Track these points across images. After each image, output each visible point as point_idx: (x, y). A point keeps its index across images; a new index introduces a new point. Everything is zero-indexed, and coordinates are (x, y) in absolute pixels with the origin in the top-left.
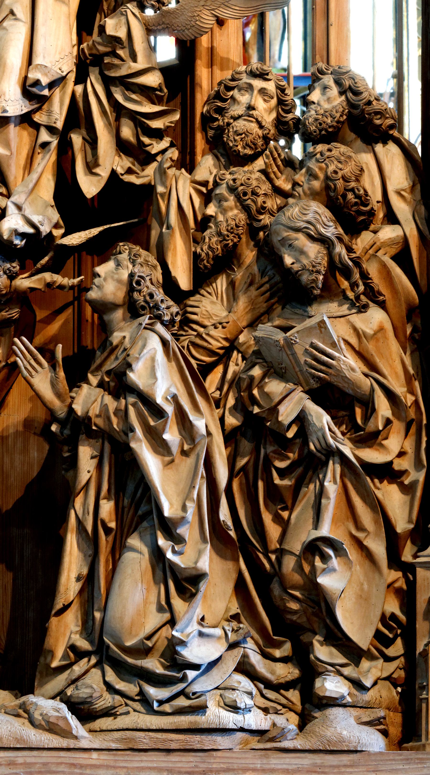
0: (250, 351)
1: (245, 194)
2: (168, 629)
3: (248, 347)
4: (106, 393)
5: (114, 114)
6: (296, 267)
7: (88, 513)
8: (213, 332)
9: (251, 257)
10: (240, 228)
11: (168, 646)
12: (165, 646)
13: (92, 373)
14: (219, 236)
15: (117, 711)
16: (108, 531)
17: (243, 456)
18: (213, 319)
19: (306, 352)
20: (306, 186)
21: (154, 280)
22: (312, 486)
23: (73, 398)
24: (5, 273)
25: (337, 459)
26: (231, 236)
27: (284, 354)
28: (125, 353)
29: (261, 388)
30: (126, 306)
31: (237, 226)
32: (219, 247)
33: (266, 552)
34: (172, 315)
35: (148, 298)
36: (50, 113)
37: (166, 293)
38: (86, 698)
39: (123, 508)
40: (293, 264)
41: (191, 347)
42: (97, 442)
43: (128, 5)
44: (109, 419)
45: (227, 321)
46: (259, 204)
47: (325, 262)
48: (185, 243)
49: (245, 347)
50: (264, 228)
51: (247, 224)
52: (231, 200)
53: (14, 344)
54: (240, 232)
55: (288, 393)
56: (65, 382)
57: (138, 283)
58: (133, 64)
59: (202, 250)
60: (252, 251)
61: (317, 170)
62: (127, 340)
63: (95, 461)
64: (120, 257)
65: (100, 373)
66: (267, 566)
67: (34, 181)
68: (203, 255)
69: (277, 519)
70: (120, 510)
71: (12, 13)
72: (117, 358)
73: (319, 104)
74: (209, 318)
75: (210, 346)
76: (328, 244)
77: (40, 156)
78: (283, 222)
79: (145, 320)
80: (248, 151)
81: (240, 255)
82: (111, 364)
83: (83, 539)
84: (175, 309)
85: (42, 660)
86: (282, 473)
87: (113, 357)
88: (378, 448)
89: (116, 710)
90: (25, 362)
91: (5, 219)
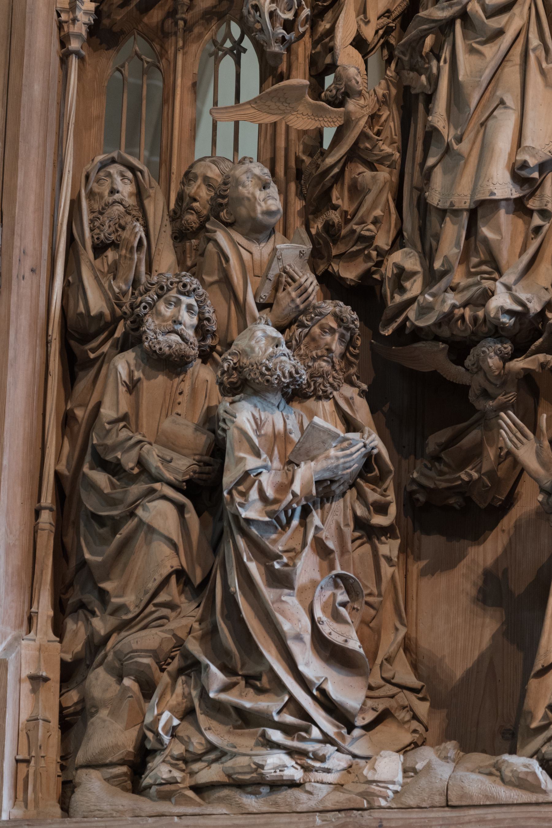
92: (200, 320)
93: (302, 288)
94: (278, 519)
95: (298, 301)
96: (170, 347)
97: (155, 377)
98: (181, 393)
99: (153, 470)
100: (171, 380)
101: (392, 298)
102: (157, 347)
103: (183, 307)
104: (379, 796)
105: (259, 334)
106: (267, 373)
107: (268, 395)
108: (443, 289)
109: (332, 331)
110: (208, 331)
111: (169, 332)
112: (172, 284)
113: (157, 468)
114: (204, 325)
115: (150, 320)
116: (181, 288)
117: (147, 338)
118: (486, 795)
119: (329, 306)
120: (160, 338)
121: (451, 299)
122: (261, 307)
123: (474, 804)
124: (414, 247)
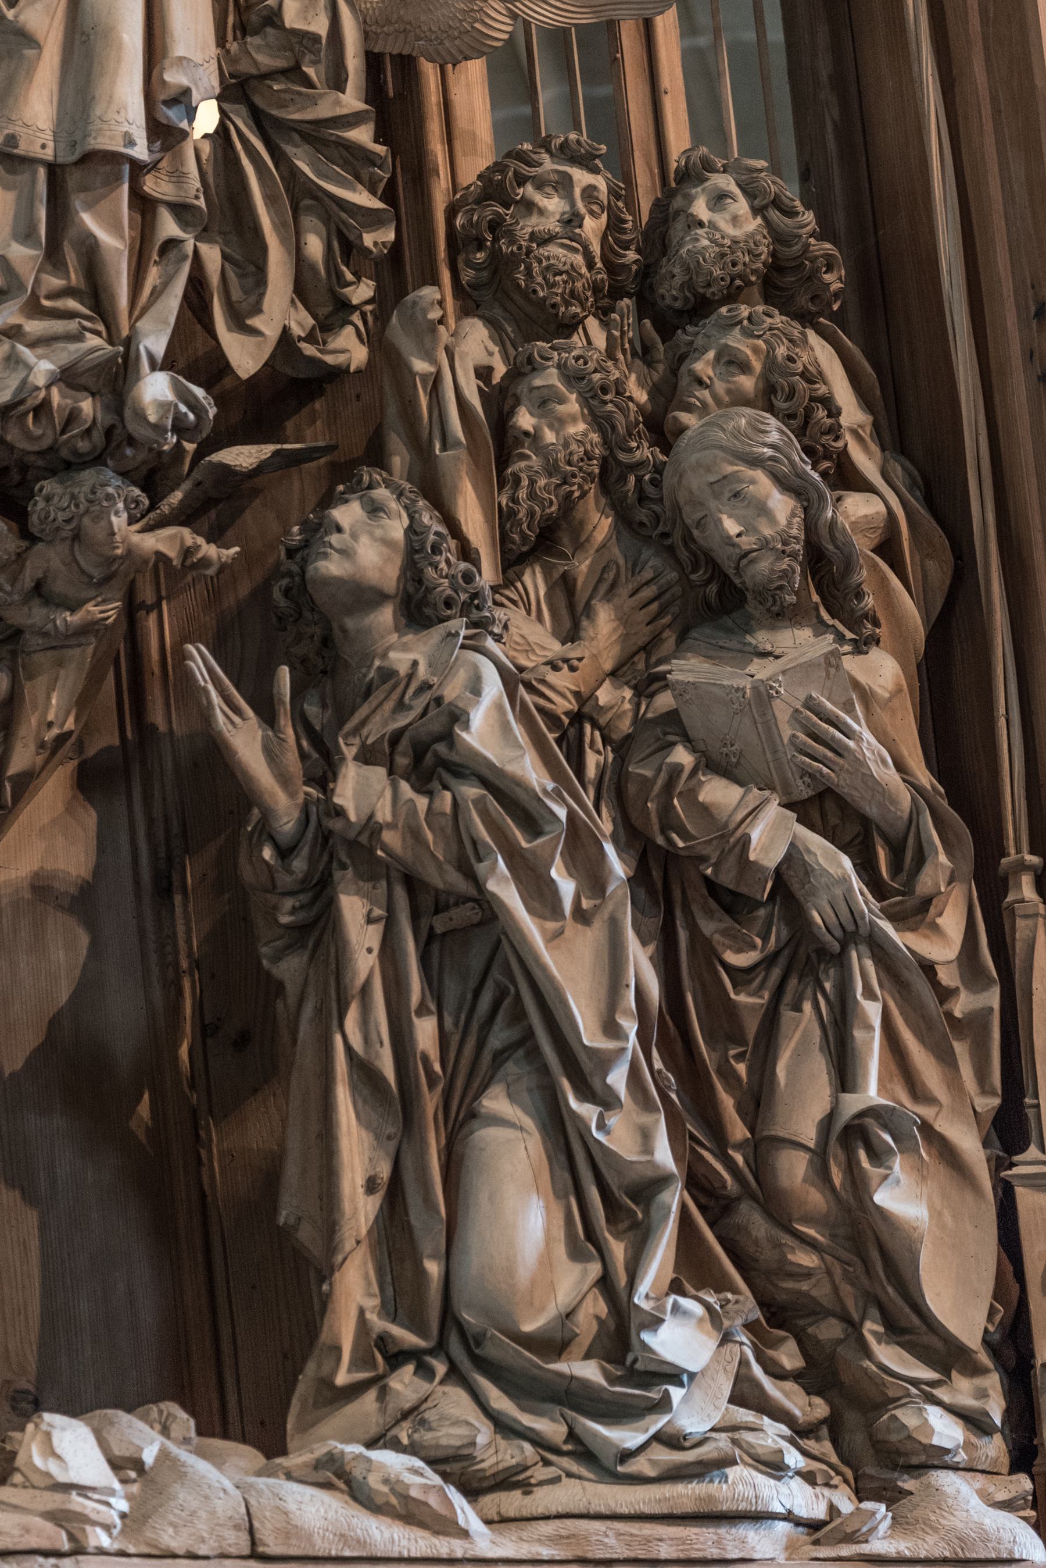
0: (625, 726)
2: (595, 1299)
3: (620, 716)
6: (747, 542)
8: (552, 677)
9: (606, 530)
10: (595, 462)
11: (598, 1335)
12: (591, 1337)
14: (550, 475)
15: (531, 1477)
18: (536, 655)
19: (796, 719)
22: (807, 1006)
24: (127, 508)
25: (864, 949)
27: (747, 721)
30: (398, 599)
32: (553, 497)
35: (461, 581)
38: (459, 1448)
40: (739, 535)
42: (374, 887)
45: (579, 656)
47: (803, 537)
49: (610, 715)
52: (572, 405)
55: (758, 803)
57: (436, 549)
60: (607, 517)
68: (522, 514)
72: (401, 706)
74: (527, 651)
75: (548, 705)
76: (808, 500)
78: (724, 443)
79: (459, 626)
81: (582, 523)
83: (365, 1102)
85: (311, 1367)
86: (741, 977)
88: (927, 932)
89: (528, 1473)
104: (95, 1523)
118: (342, 1535)
123: (315, 1554)
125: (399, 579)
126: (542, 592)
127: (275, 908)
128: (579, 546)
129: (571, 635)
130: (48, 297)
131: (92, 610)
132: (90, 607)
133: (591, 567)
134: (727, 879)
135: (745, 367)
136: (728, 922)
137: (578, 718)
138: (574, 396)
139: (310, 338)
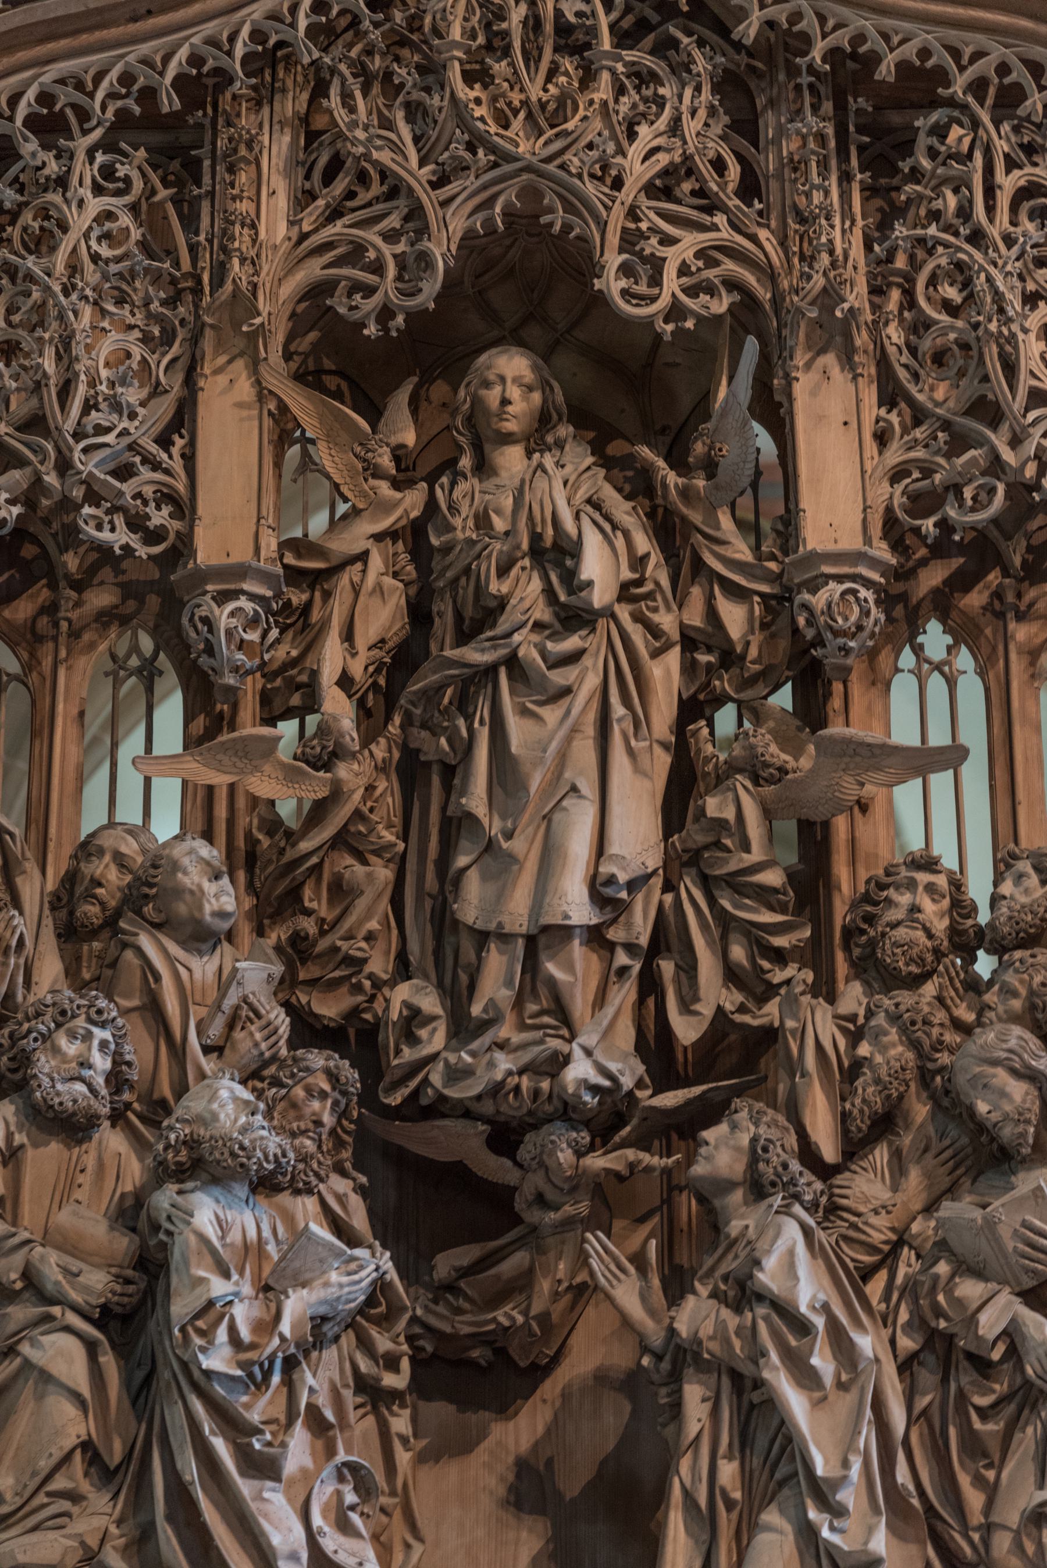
0: (929, 1245)
1: (913, 1023)
3: (925, 1240)
4: (723, 1306)
5: (720, 930)
7: (700, 1480)
8: (873, 1220)
13: (700, 1280)
16: (730, 1505)
17: (924, 1394)
20: (1001, 1009)
21: (787, 1147)
22: (1030, 1430)
23: (673, 1318)
24: (569, 1145)
26: (895, 1083)
28: (748, 1248)
29: (949, 1292)
31: (903, 1069)
33: (965, 1529)
34: (815, 1193)
35: (780, 1169)
36: (629, 925)
37: (803, 1163)
39: (751, 1471)
41: (842, 1243)
43: (738, 776)
44: (727, 1342)
46: (934, 1037)
48: (828, 1098)
49: (920, 1239)
50: (942, 1070)
51: (918, 1067)
52: (893, 1035)
53: (584, 1240)
54: (908, 1077)
56: (661, 1293)
57: (765, 1150)
58: (745, 856)
59: (853, 1105)
61: (1017, 984)
62: (751, 1230)
63: (708, 1406)
64: (736, 1116)
65: (712, 1281)
66: (968, 1550)
67: (610, 1017)
68: (856, 1112)
69: (979, 1481)
70: (747, 1475)
71: (574, 789)
72: (736, 1257)
73: (1012, 898)
75: (869, 1240)
77: (616, 986)
80: (914, 969)
81: (908, 1111)
82: (729, 1265)
84: (819, 1186)
86: (984, 1414)
87: (730, 1256)
90: (603, 1268)
91: (570, 1066)
92: (114, 1062)
93: (271, 1027)
94: (251, 1375)
95: (264, 1046)
96: (75, 1101)
97: (47, 1144)
98: (82, 1171)
99: (49, 1287)
100: (69, 1149)
101: (398, 1052)
102: (57, 1100)
103: (96, 1043)
105: (224, 1094)
106: (241, 1153)
107: (234, 1184)
108: (487, 1046)
109: (323, 1095)
110: (127, 1080)
111: (72, 1079)
112: (79, 1007)
113: (57, 1283)
114: (121, 1071)
115: (43, 1059)
116: (95, 1016)
117: (39, 1086)
119: (317, 1059)
120: (59, 1087)
121: (504, 1063)
122: (207, 1050)
124: (426, 977)
125: (745, 1172)
126: (885, 1161)
127: (656, 1394)
128: (907, 1127)
129: (895, 1188)
130: (530, 1017)
131: (568, 1209)
132: (567, 1208)
133: (912, 1140)
134: (972, 1348)
135: (1015, 994)
136: (975, 1375)
137: (897, 1246)
138: (894, 1030)
139: (742, 1009)
